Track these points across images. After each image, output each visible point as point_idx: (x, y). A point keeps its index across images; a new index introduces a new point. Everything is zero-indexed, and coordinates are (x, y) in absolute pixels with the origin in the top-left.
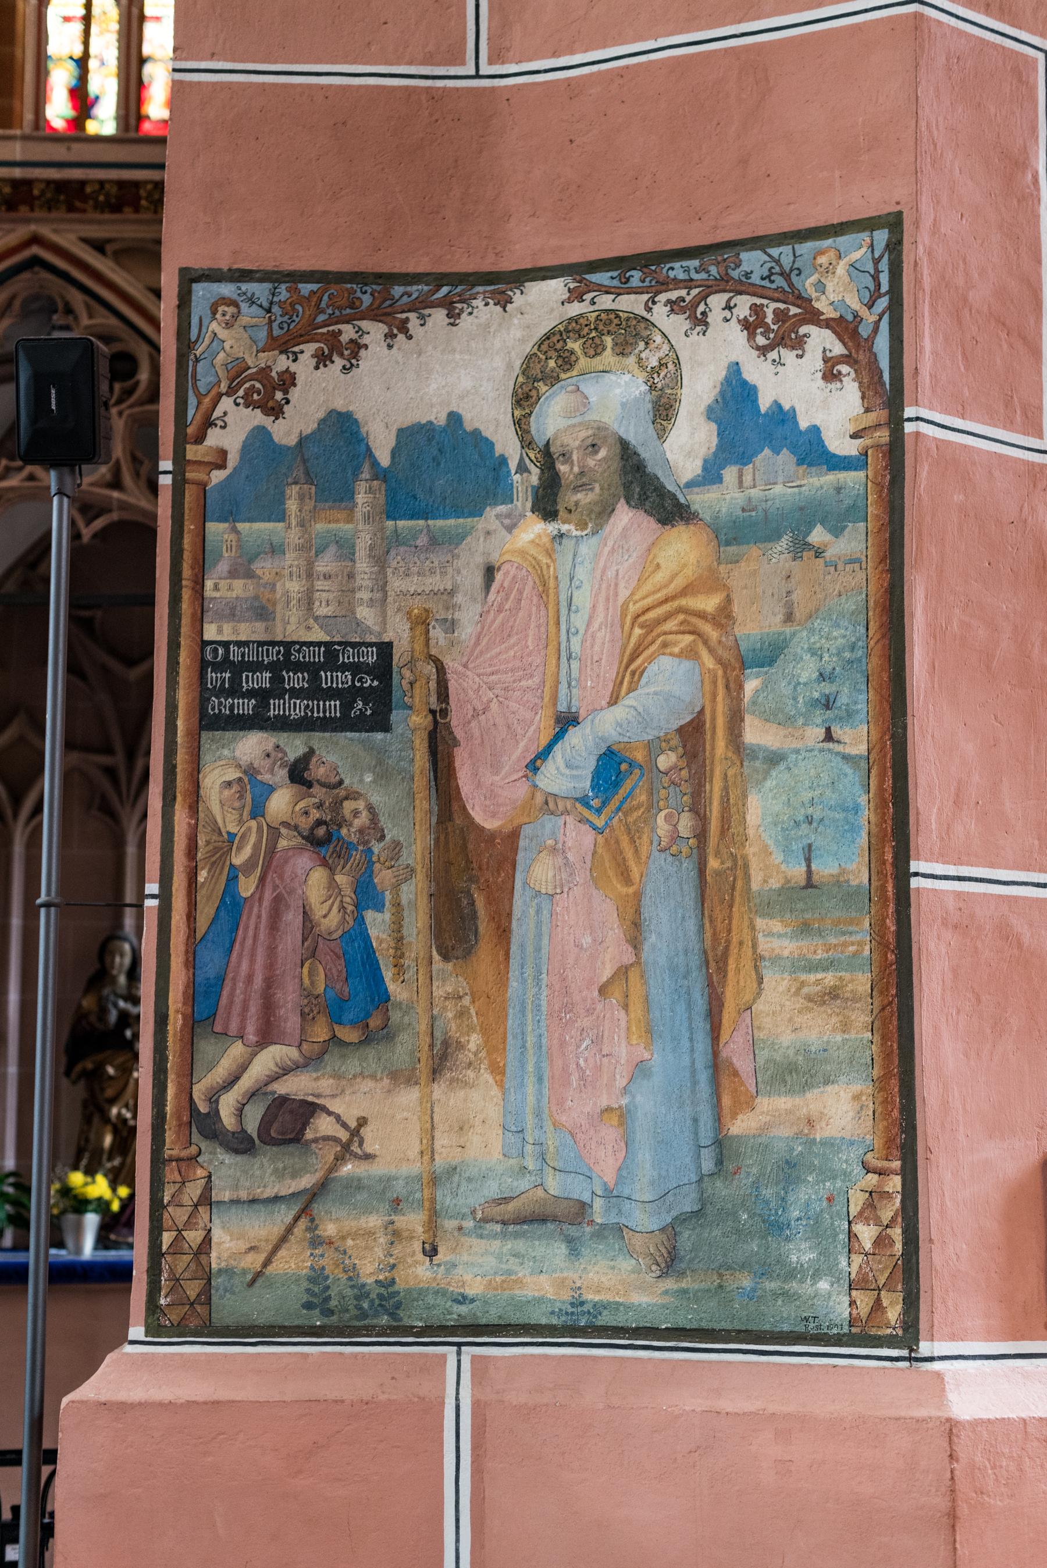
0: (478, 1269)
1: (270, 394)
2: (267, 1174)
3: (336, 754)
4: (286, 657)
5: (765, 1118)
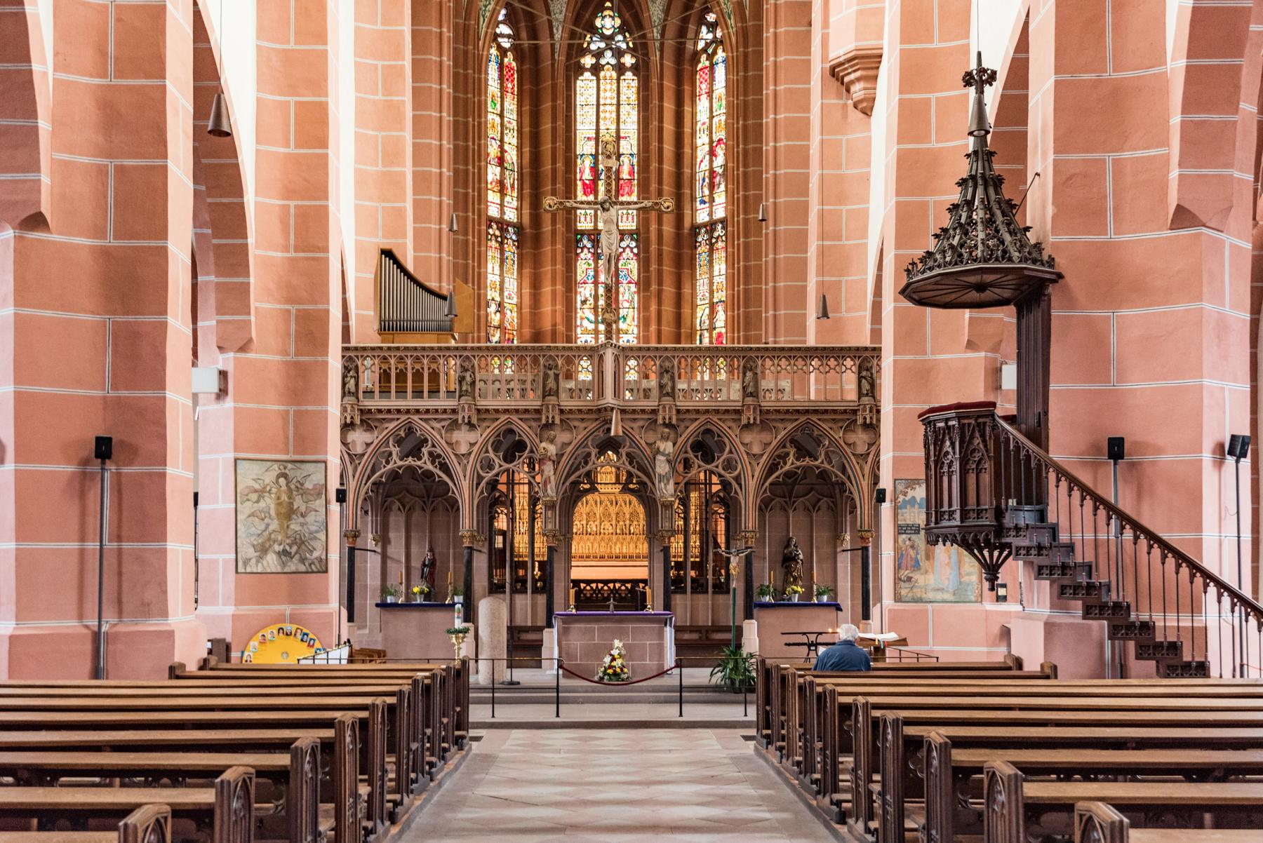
0: (931, 596)
1: (905, 494)
2: (907, 585)
3: (914, 537)
4: (908, 526)
5: (966, 579)
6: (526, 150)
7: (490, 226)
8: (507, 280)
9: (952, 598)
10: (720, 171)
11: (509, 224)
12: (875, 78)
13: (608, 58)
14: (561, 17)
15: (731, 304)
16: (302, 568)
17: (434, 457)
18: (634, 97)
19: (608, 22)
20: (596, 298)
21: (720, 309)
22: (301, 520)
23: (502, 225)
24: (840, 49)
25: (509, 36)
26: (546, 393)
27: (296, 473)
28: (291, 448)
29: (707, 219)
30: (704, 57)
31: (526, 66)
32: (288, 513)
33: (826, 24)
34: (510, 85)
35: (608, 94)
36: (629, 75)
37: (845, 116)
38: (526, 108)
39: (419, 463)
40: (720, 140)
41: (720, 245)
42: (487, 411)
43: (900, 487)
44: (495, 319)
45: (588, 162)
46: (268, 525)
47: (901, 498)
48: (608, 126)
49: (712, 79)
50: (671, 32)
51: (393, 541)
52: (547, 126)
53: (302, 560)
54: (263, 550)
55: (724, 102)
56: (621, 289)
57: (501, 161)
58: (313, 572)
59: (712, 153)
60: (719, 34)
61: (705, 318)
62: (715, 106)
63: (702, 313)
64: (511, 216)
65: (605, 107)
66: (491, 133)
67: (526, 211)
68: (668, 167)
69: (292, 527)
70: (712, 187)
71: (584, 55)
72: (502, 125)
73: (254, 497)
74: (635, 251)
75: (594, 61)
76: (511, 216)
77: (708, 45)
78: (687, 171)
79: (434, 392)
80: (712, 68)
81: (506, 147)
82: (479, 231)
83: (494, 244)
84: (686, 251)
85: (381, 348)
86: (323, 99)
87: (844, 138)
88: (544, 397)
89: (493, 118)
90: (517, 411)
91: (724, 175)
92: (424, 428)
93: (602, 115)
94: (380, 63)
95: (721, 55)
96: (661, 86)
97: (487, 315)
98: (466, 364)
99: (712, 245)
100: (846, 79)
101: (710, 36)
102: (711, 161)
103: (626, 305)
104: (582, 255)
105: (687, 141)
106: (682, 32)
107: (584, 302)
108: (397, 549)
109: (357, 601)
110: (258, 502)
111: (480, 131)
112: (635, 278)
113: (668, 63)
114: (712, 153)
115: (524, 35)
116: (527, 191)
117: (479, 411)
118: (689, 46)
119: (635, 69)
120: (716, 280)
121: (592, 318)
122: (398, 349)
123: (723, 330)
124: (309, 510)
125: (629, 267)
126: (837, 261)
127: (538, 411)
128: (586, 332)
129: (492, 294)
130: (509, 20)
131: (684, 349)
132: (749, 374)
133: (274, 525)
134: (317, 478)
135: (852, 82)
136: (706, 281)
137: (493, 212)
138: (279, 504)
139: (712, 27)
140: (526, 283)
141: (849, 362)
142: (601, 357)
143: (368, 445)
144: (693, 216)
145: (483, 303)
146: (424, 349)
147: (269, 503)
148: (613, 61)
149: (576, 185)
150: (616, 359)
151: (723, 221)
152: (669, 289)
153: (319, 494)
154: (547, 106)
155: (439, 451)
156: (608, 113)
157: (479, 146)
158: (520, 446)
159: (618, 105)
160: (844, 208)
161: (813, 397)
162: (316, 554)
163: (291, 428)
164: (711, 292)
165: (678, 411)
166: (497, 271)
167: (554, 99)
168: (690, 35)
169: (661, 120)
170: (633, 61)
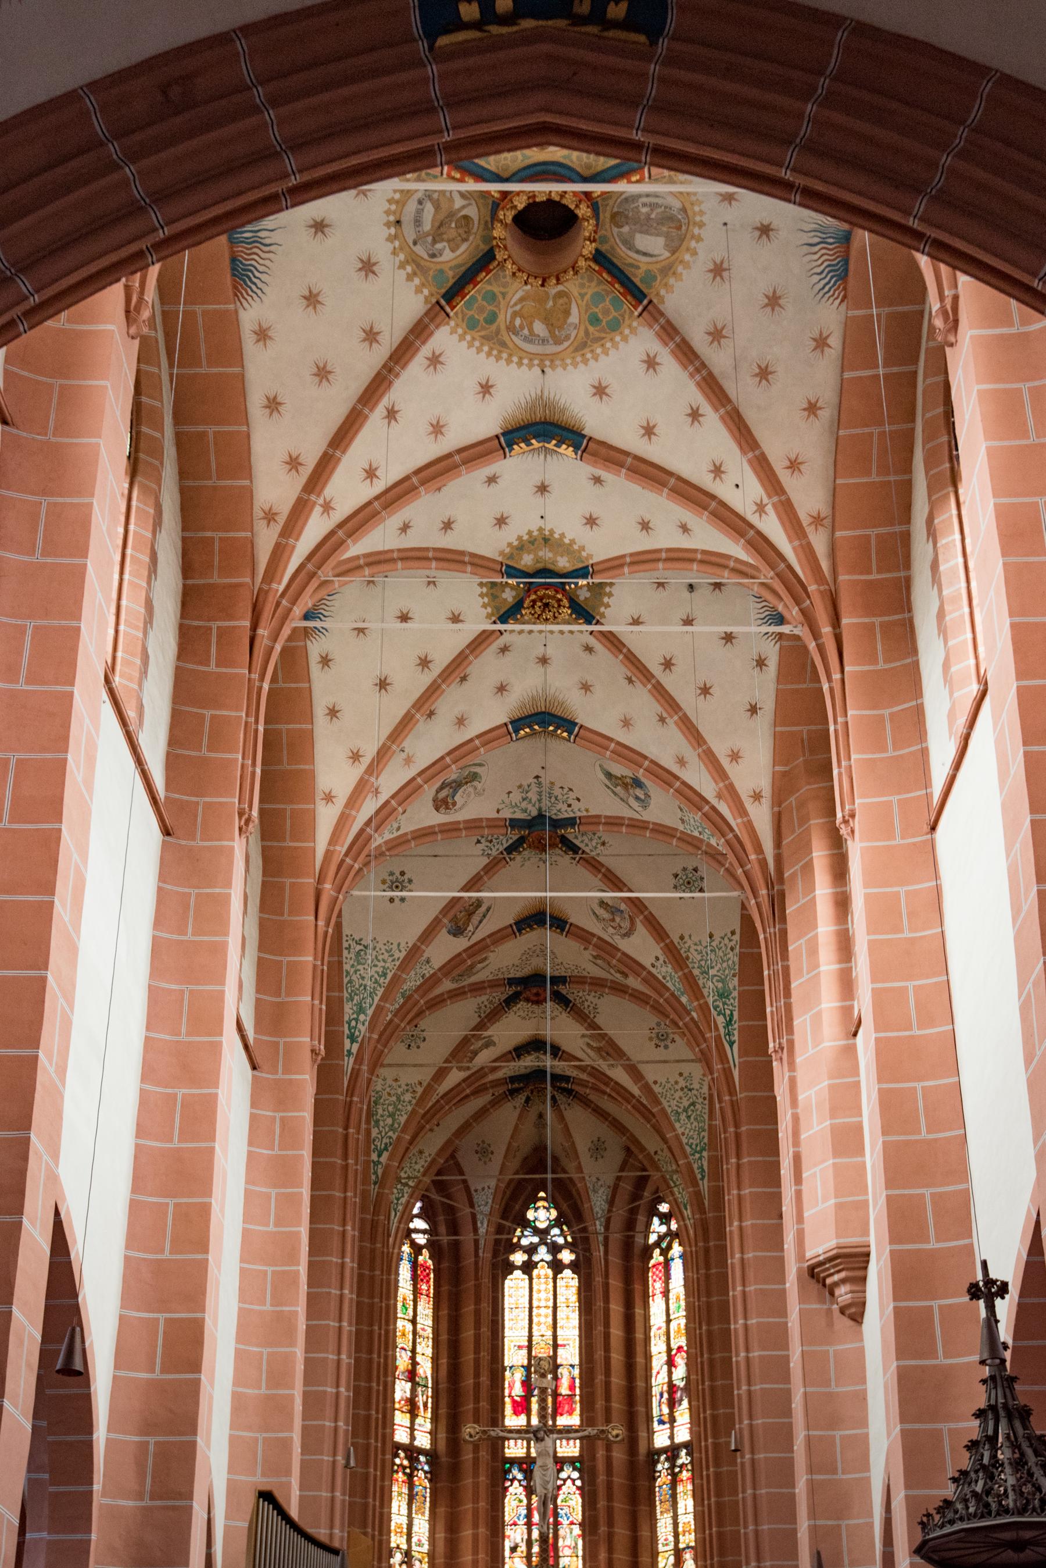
6: (444, 1361)
7: (397, 1455)
10: (682, 1384)
11: (421, 1451)
13: (543, 1254)
18: (574, 1298)
20: (529, 1543)
23: (412, 1452)
25: (424, 1232)
29: (668, 1443)
30: (657, 1251)
31: (445, 1265)
34: (424, 1287)
35: (543, 1295)
36: (567, 1273)
38: (444, 1312)
40: (680, 1349)
41: (685, 1475)
45: (519, 1376)
48: (542, 1331)
50: (617, 1224)
52: (468, 1334)
55: (683, 1303)
57: (412, 1375)
60: (674, 1226)
62: (672, 1307)
64: (423, 1441)
65: (539, 1311)
66: (400, 1342)
67: (442, 1435)
68: (617, 1380)
70: (672, 1404)
71: (513, 1252)
72: (415, 1333)
74: (579, 1483)
75: (525, 1257)
76: (423, 1441)
77: (661, 1238)
78: (640, 1384)
80: (667, 1264)
81: (419, 1358)
83: (400, 1476)
89: (403, 1325)
91: (687, 1389)
93: (535, 1319)
95: (677, 1250)
96: (606, 1286)
101: (663, 1229)
102: (670, 1373)
103: (567, 1552)
105: (639, 1349)
106: (630, 1225)
107: (514, 1549)
113: (615, 1260)
114: (671, 1363)
115: (442, 1229)
116: (443, 1411)
118: (639, 1239)
120: (682, 1519)
125: (571, 1503)
130: (423, 1215)
136: (670, 1521)
137: (401, 1436)
148: (549, 1258)
149: (503, 1403)
151: (686, 1445)
152: (621, 1531)
154: (469, 1309)
156: (542, 1317)
166: (404, 1511)
167: (478, 1301)
168: (640, 1226)
169: (607, 1325)
170: (573, 1257)
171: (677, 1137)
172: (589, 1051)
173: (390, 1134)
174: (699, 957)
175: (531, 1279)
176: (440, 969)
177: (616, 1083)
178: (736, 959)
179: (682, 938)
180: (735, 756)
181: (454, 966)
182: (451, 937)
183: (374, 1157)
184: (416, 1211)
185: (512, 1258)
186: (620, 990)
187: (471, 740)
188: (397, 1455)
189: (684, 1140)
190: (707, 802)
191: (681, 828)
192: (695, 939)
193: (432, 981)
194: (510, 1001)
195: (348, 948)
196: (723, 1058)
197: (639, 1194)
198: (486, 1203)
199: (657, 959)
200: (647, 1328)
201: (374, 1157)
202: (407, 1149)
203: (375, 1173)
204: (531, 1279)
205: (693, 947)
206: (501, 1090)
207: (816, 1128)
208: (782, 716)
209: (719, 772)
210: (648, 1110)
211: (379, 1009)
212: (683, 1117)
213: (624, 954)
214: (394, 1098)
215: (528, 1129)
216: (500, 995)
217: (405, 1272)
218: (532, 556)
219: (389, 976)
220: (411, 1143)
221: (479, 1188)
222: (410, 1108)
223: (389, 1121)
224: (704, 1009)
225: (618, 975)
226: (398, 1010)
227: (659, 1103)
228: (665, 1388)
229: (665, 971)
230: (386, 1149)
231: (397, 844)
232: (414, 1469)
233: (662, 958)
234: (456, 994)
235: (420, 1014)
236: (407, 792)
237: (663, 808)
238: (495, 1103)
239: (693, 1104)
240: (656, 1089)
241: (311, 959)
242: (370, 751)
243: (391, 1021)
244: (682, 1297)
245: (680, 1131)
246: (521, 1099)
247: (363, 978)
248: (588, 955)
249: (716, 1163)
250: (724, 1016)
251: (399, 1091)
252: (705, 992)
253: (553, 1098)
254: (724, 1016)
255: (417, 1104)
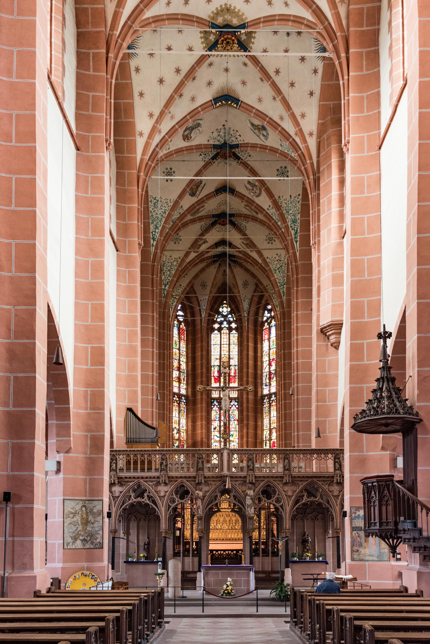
0: (367, 558)
1: (355, 513)
2: (356, 553)
3: (359, 532)
4: (357, 527)
5: (382, 551)
6: (190, 364)
7: (174, 397)
8: (181, 419)
9: (376, 559)
10: (274, 372)
11: (182, 395)
12: (340, 333)
13: (225, 324)
14: (205, 308)
15: (278, 429)
16: (92, 547)
17: (149, 497)
18: (236, 341)
19: (225, 310)
20: (220, 427)
21: (274, 431)
22: (92, 525)
23: (180, 396)
24: (325, 321)
25: (182, 316)
26: (198, 470)
27: (90, 505)
28: (88, 494)
29: (268, 393)
30: (266, 324)
31: (190, 329)
32: (86, 522)
33: (319, 310)
34: (183, 337)
35: (225, 340)
36: (234, 332)
37: (327, 350)
38: (190, 346)
39: (143, 500)
40: (273, 359)
41: (274, 404)
42: (173, 477)
43: (353, 511)
44: (176, 436)
45: (216, 369)
46: (77, 528)
47: (353, 515)
48: (225, 352)
49: (270, 333)
50: (252, 313)
51: (131, 534)
52: (199, 354)
53: (92, 543)
54: (75, 539)
55: (275, 343)
56: (231, 423)
57: (179, 369)
58: (97, 548)
59: (270, 365)
60: (273, 314)
61: (267, 435)
63: (266, 433)
64: (183, 392)
65: (224, 346)
67: (190, 390)
68: (251, 371)
69: (88, 528)
70: (270, 379)
71: (214, 324)
72: (179, 353)
73: (71, 516)
74: (237, 406)
75: (219, 326)
76: (183, 392)
77: (268, 319)
78: (259, 372)
79: (150, 469)
80: (270, 328)
81: (181, 363)
82: (170, 399)
83: (176, 404)
84: (259, 406)
85: (127, 451)
86: (103, 345)
87: (327, 359)
88: (197, 471)
89: (175, 351)
90: (185, 477)
91: (275, 374)
92: (145, 484)
93: (222, 349)
94: (127, 329)
95: (273, 323)
96: (248, 336)
97: (173, 434)
98: (163, 457)
99: (270, 404)
100: (328, 334)
101: (269, 315)
102: (270, 368)
103: (233, 429)
104: (214, 409)
105: (259, 359)
106: (257, 314)
107: (215, 429)
108: (133, 537)
109: (116, 560)
110: (73, 518)
111: (170, 356)
112: (237, 418)
114: (270, 365)
115: (189, 315)
116: (190, 381)
117: (169, 477)
118: (260, 319)
119: (236, 329)
120: (272, 418)
121: (218, 435)
122: (134, 451)
123: (275, 440)
124: (95, 521)
126: (325, 411)
127: (194, 477)
128: (216, 441)
129: (175, 425)
130: (182, 309)
131: (258, 450)
132: (286, 461)
133: (80, 528)
134: (99, 507)
135: (330, 335)
136: (268, 419)
137: (176, 390)
138: (82, 519)
139: (270, 311)
140: (190, 420)
141: (330, 456)
142: (222, 454)
143: (121, 492)
144: (262, 391)
145: (171, 430)
146: (145, 451)
147: (78, 518)
148: (227, 326)
149: (211, 379)
150: (229, 454)
151: (275, 393)
152: (251, 423)
153: (100, 514)
154: (199, 345)
155: (151, 495)
157: (170, 362)
158: (187, 492)
159: (229, 344)
160: (327, 389)
161: (314, 471)
162: (98, 540)
163: (88, 485)
164: (270, 424)
165: (256, 477)
166: (177, 416)
167: (202, 342)
168: (260, 314)
169: (248, 351)
170: (236, 326)
171: (275, 279)
172: (243, 245)
173: (169, 278)
174: (286, 206)
175: (221, 334)
176: (186, 210)
177: (253, 258)
178: (300, 206)
179: (279, 197)
180: (303, 116)
181: (192, 209)
182: (190, 197)
183: (163, 287)
184: (179, 308)
185: (214, 326)
186: (255, 219)
187: (197, 108)
188: (174, 397)
189: (278, 281)
190: (291, 137)
191: (280, 148)
192: (284, 198)
193: (183, 216)
194: (213, 224)
195: (151, 201)
196: (293, 248)
197: (260, 302)
198: (204, 306)
199: (270, 206)
200: (262, 352)
201: (163, 287)
202: (175, 284)
203: (164, 293)
204: (221, 334)
205: (284, 201)
206: (210, 261)
207: (327, 275)
208: (323, 97)
209: (297, 123)
210: (265, 269)
211: (164, 227)
212: (277, 271)
213: (257, 204)
214: (170, 264)
215: (220, 276)
216: (209, 221)
217: (176, 331)
218: (222, 18)
219: (167, 213)
220: (177, 281)
221: (202, 299)
222: (176, 268)
223: (168, 273)
224: (287, 227)
225: (254, 213)
226: (171, 228)
227: (268, 266)
228: (268, 373)
229: (272, 212)
230: (167, 284)
231: (169, 155)
232: (180, 401)
233: (271, 206)
234: (193, 221)
235: (179, 229)
236: (172, 132)
237: (273, 140)
238: (208, 266)
239: (281, 266)
240: (268, 260)
241: (137, 205)
242: (157, 113)
243: (168, 232)
244: (275, 341)
245: (276, 277)
246: (217, 265)
247: (157, 214)
248: (243, 204)
249: (289, 290)
250: (294, 230)
251: (172, 261)
252: (287, 220)
253: (229, 264)
254: (294, 230)
255: (179, 266)
